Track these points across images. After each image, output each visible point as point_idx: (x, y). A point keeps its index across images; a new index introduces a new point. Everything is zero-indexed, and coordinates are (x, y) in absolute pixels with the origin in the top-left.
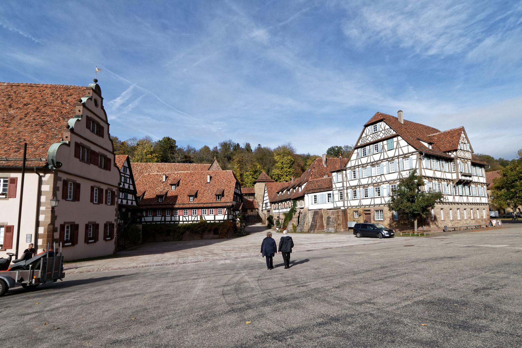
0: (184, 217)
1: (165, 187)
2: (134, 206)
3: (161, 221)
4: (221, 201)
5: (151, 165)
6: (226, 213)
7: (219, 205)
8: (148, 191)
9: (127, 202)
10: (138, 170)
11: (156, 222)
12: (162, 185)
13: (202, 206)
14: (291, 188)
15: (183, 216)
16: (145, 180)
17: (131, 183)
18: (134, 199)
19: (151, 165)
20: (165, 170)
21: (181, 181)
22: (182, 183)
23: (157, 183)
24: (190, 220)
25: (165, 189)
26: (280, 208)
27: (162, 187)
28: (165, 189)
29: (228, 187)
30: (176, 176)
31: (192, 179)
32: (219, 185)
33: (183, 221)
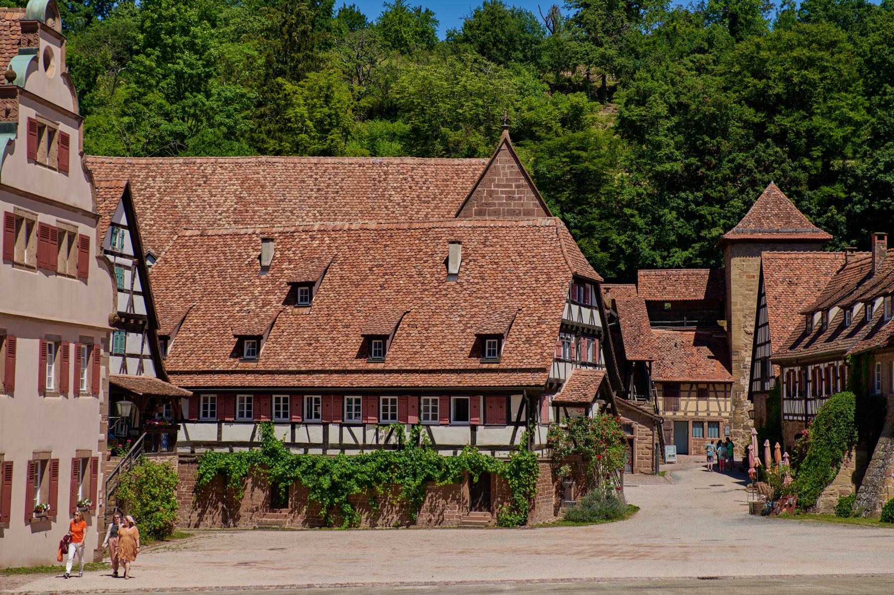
0: (345, 429)
1: (267, 293)
2: (150, 383)
3: (250, 444)
4: (503, 365)
5: (209, 171)
6: (523, 419)
7: (492, 383)
8: (198, 309)
9: (124, 367)
10: (152, 195)
11: (231, 444)
12: (258, 282)
13: (421, 384)
14: (855, 302)
15: (341, 426)
16: (187, 257)
17: (138, 287)
18: (147, 351)
19: (209, 171)
20: (270, 193)
21: (335, 268)
22: (342, 278)
23: (235, 275)
24: (371, 439)
25: (269, 303)
26: (809, 396)
27: (256, 293)
28: (269, 303)
29: (535, 300)
30: (316, 243)
31: (383, 260)
32: (496, 289)
33: (343, 447)
